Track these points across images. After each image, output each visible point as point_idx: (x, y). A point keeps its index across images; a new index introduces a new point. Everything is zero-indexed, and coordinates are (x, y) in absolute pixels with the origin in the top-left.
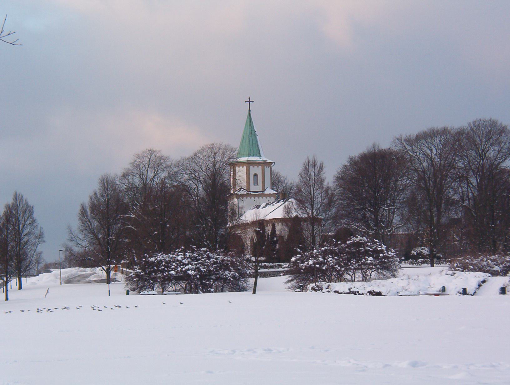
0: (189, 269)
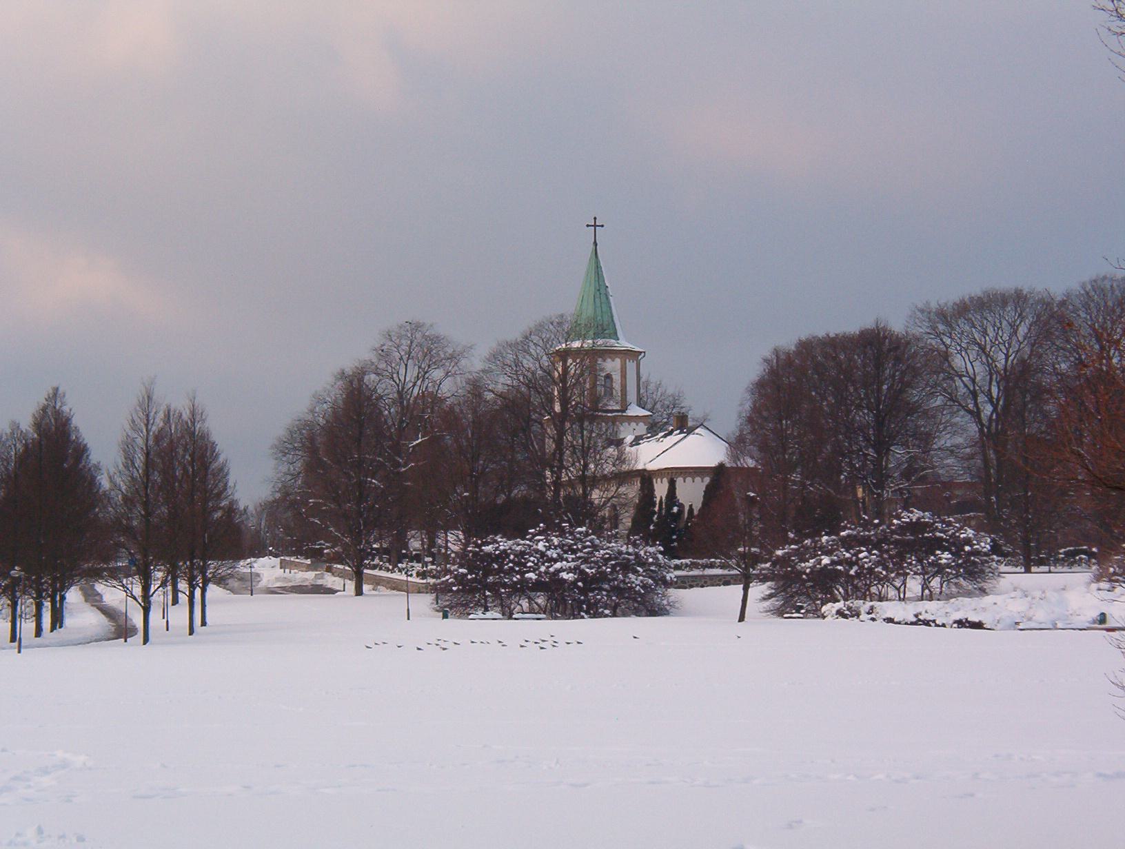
0: (561, 570)
